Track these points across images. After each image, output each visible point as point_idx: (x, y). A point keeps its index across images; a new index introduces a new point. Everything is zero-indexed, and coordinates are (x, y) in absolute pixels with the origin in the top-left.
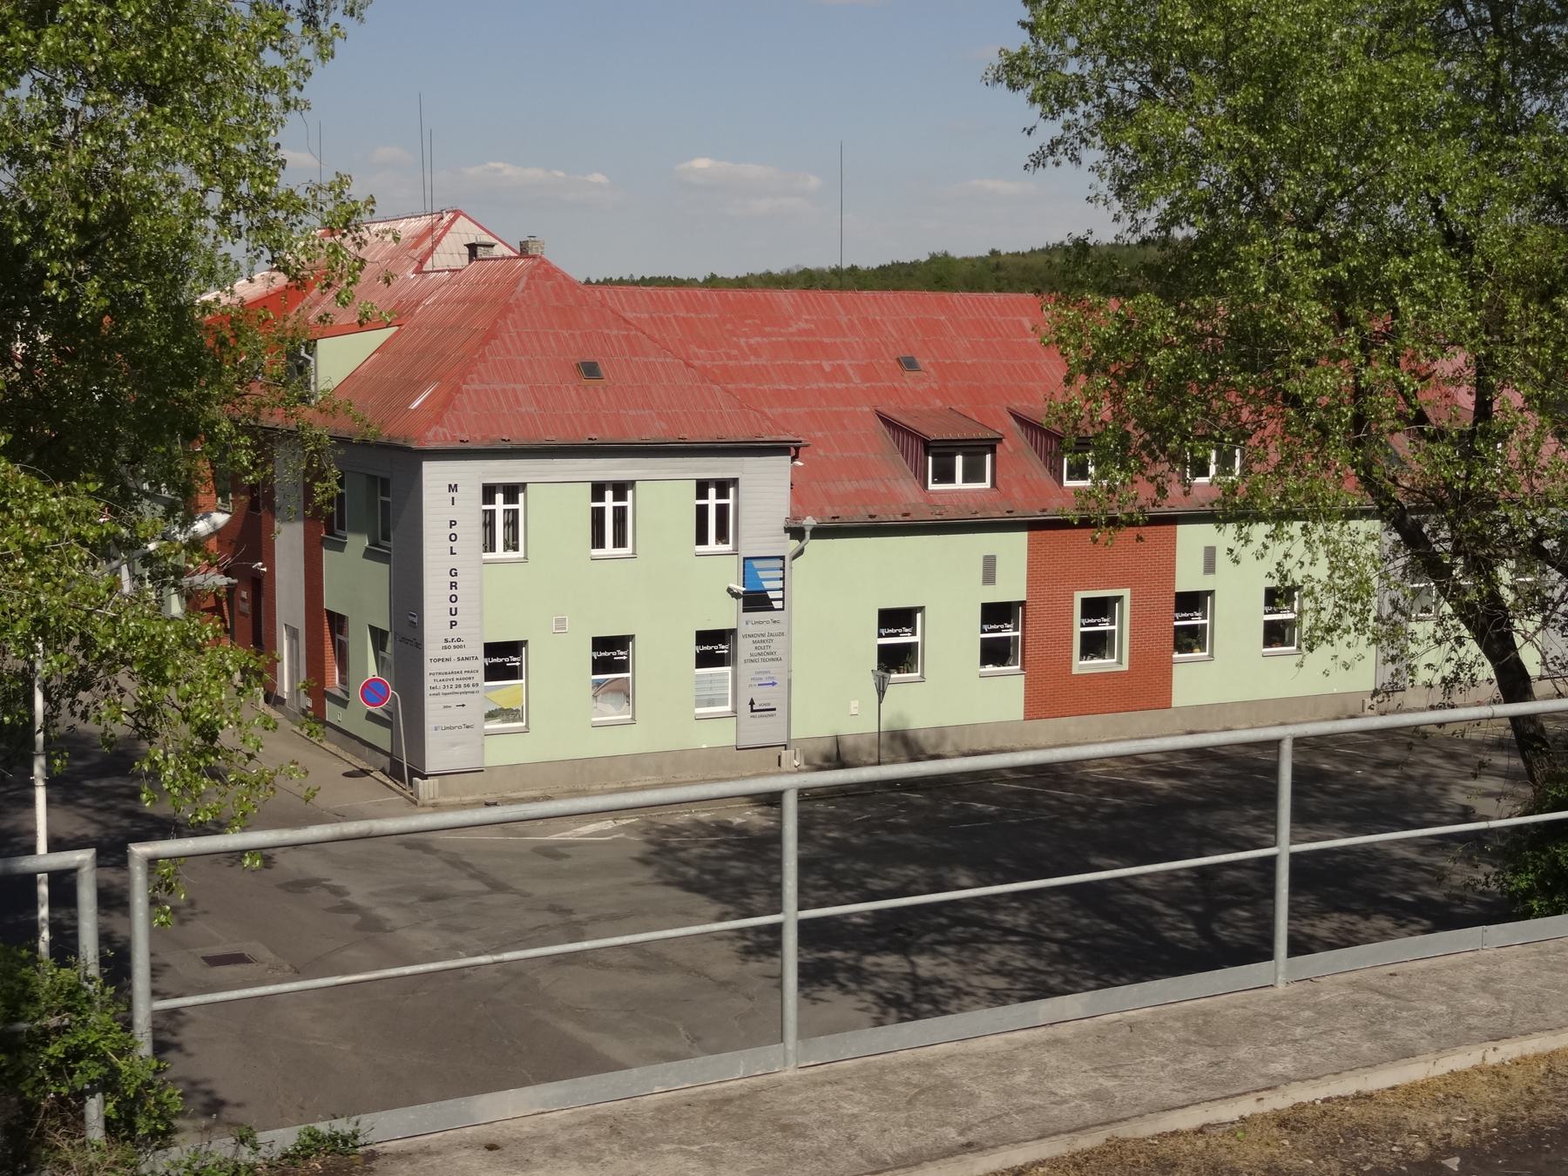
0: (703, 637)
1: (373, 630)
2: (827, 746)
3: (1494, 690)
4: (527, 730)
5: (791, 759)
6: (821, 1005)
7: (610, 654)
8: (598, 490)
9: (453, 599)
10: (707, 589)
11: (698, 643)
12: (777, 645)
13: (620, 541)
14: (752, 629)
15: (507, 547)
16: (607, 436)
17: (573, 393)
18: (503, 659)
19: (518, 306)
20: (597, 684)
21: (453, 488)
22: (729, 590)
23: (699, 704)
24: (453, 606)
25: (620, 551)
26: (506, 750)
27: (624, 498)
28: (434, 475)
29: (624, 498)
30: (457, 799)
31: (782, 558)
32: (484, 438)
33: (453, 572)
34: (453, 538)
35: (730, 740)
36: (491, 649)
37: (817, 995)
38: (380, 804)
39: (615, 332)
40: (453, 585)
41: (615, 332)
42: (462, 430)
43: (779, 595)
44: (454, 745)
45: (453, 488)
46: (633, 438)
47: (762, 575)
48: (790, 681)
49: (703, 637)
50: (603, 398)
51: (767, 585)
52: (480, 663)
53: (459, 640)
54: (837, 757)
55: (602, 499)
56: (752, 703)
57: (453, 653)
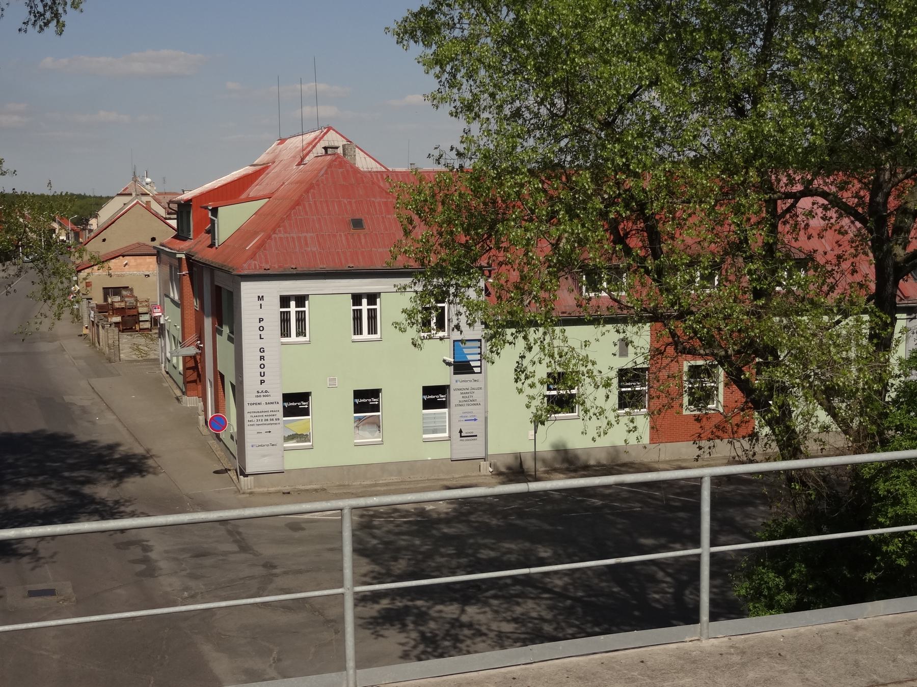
0: (427, 390)
1: (232, 384)
2: (510, 461)
3: (775, 448)
4: (311, 448)
5: (486, 469)
6: (380, 639)
7: (366, 401)
8: (357, 299)
9: (262, 366)
10: (432, 362)
11: (284, 401)
12: (478, 395)
13: (301, 332)
14: (460, 385)
15: (298, 334)
16: (362, 265)
17: (344, 238)
18: (296, 403)
19: (318, 185)
20: (359, 419)
21: (260, 298)
22: (444, 361)
23: (426, 432)
24: (262, 371)
25: (301, 339)
26: (297, 459)
27: (375, 304)
28: (249, 291)
29: (375, 304)
30: (265, 490)
31: (480, 341)
32: (280, 267)
33: (262, 350)
34: (261, 329)
35: (447, 455)
36: (287, 397)
37: (382, 632)
38: (219, 492)
39: (378, 200)
40: (262, 358)
41: (378, 200)
42: (267, 262)
43: (478, 363)
44: (264, 456)
45: (260, 298)
46: (300, 270)
47: (466, 351)
48: (486, 419)
49: (427, 390)
50: (363, 241)
51: (469, 357)
52: (280, 407)
53: (266, 392)
54: (516, 471)
55: (360, 304)
56: (461, 432)
57: (263, 400)
